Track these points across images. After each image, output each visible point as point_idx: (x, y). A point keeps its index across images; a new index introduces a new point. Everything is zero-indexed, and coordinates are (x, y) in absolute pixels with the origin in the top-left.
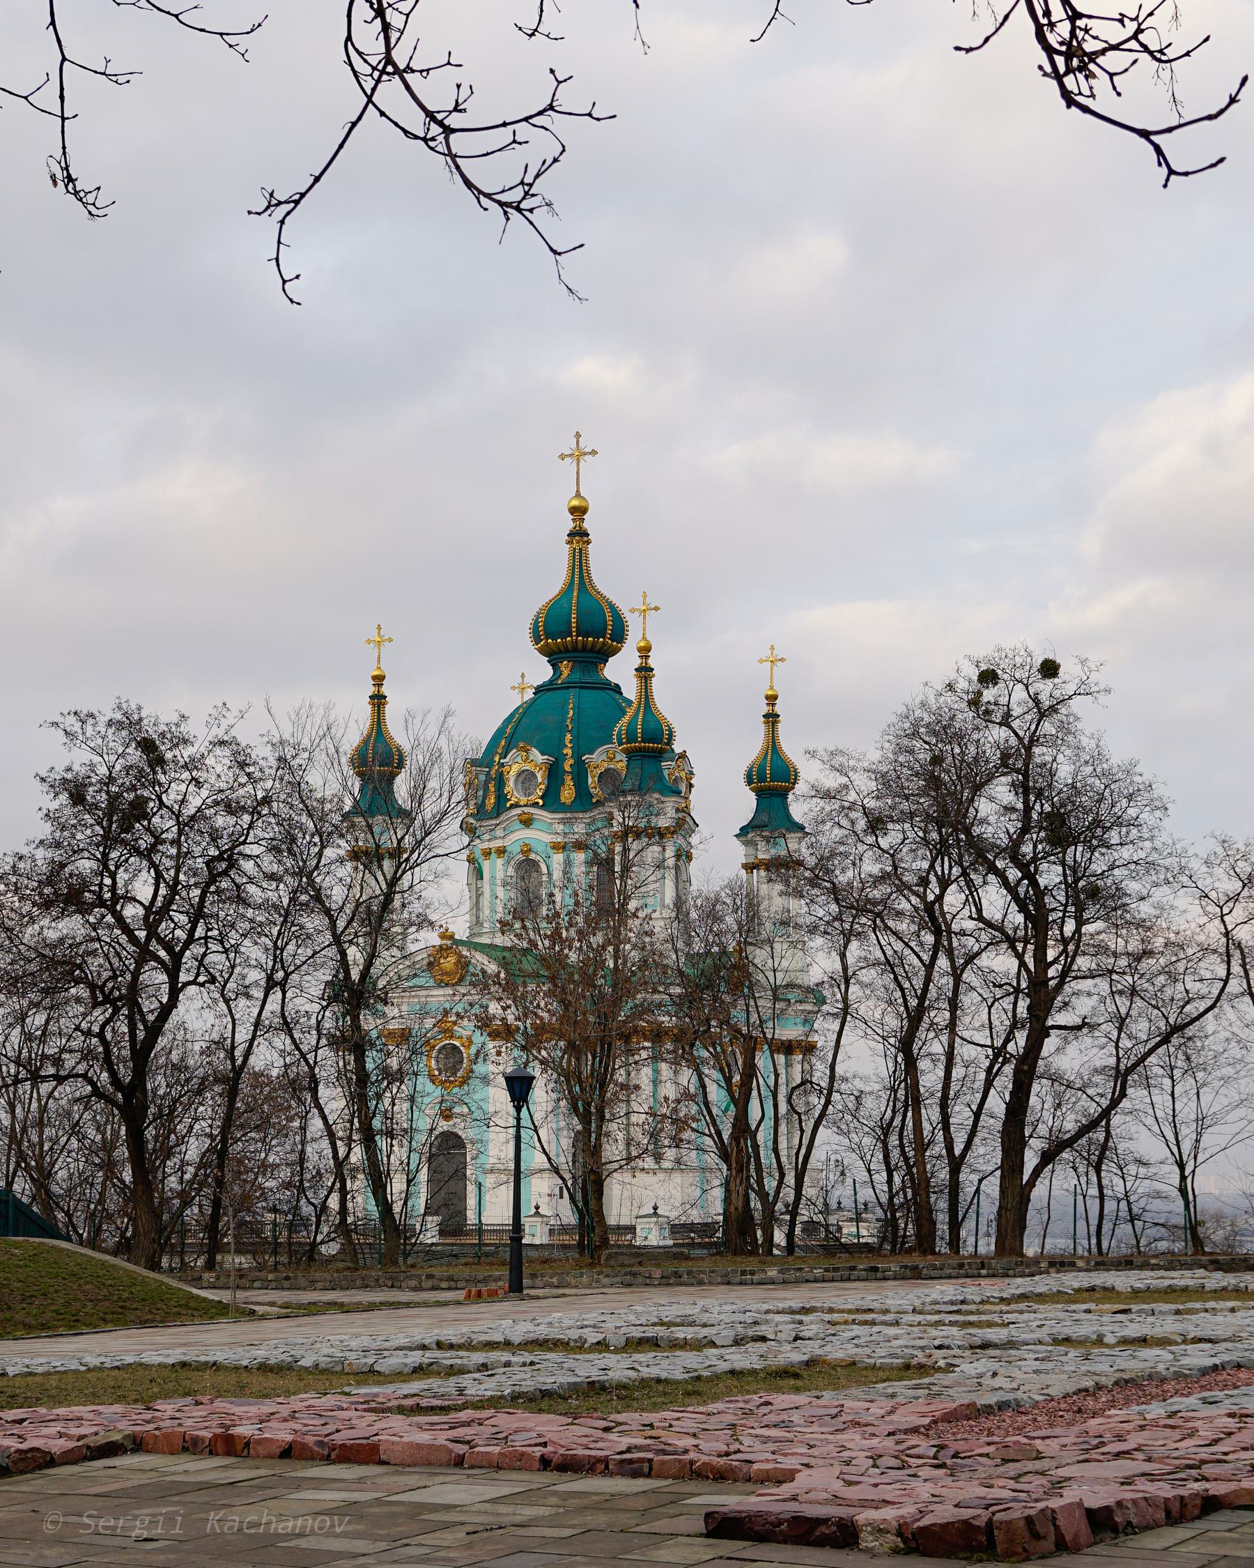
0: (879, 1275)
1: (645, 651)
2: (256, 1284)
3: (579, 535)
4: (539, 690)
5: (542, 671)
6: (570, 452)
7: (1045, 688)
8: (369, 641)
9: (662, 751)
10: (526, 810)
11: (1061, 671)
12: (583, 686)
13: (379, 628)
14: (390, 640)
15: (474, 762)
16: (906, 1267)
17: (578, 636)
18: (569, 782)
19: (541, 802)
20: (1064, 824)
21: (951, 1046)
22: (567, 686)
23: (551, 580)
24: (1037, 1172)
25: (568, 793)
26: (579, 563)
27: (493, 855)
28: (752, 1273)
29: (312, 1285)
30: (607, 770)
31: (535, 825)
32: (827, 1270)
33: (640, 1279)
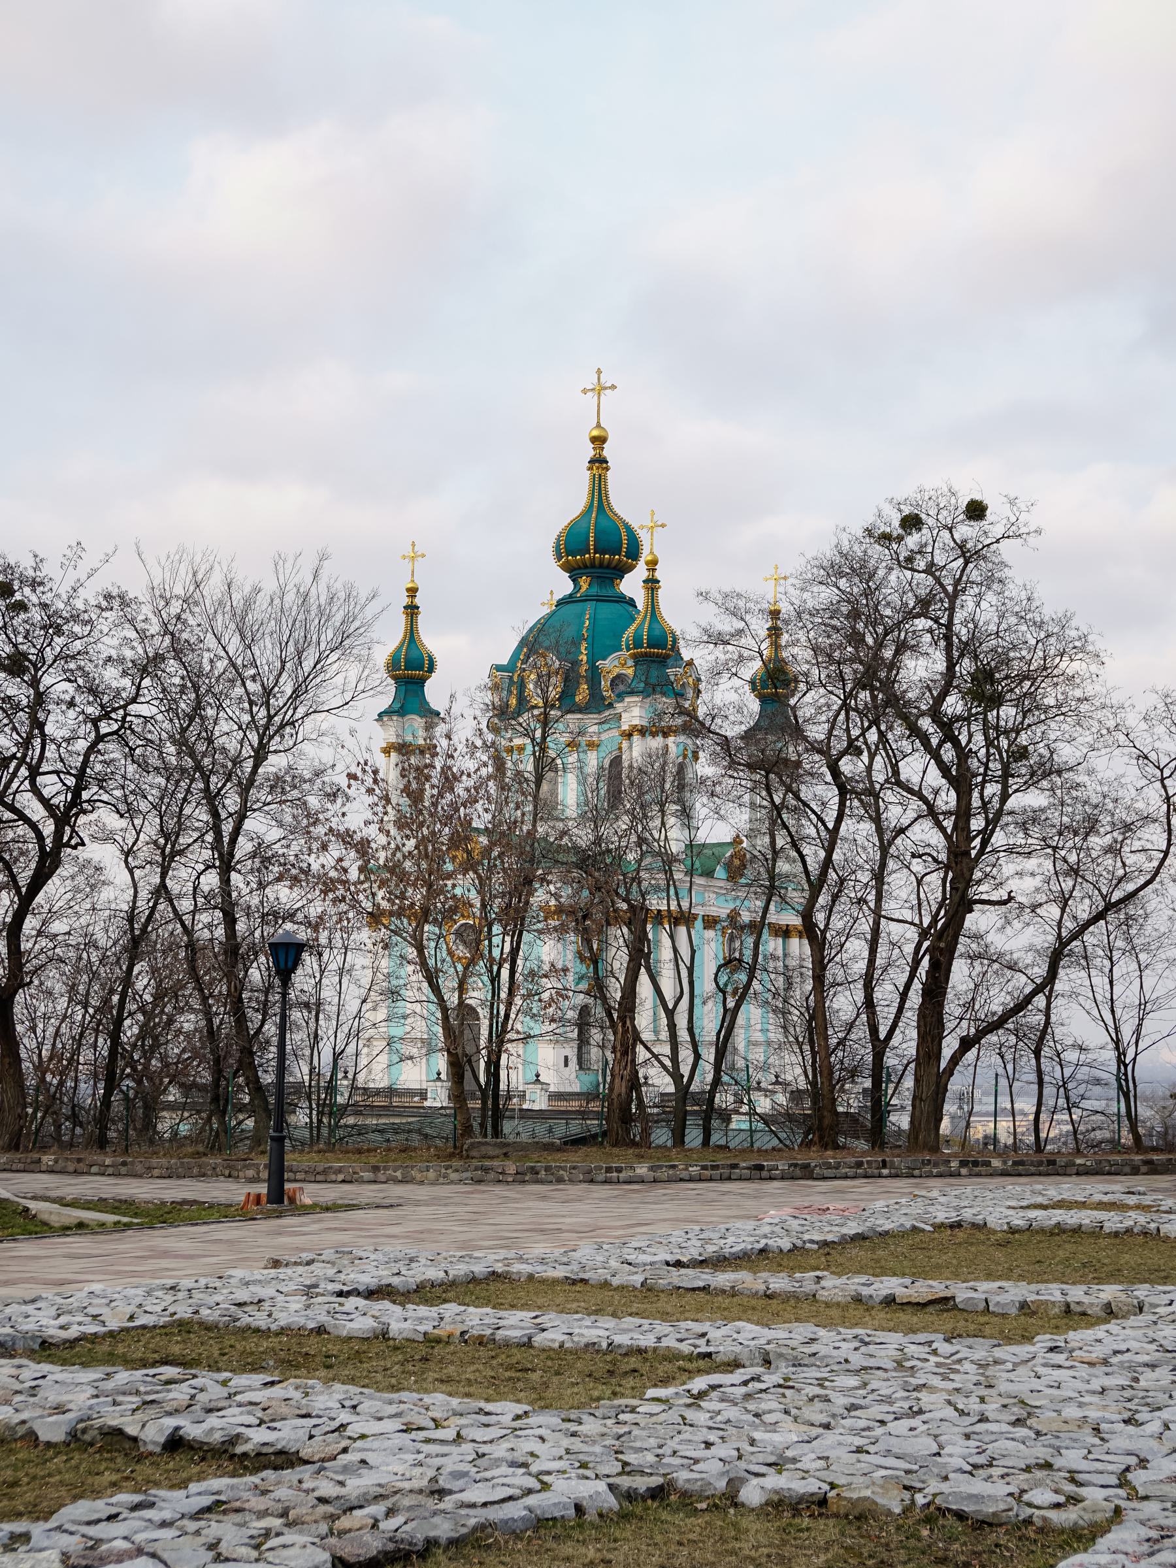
0: (765, 1174)
1: (652, 564)
2: (94, 1169)
3: (599, 462)
4: (561, 603)
5: (564, 585)
7: (967, 531)
8: (404, 557)
9: (667, 656)
11: (988, 512)
12: (599, 599)
13: (413, 544)
14: (423, 556)
15: (499, 668)
16: (796, 1165)
20: (988, 682)
21: (877, 924)
22: (585, 599)
24: (955, 1060)
25: (582, 693)
26: (599, 489)
28: (619, 1170)
29: (147, 1173)
32: (704, 1168)
33: (492, 1175)
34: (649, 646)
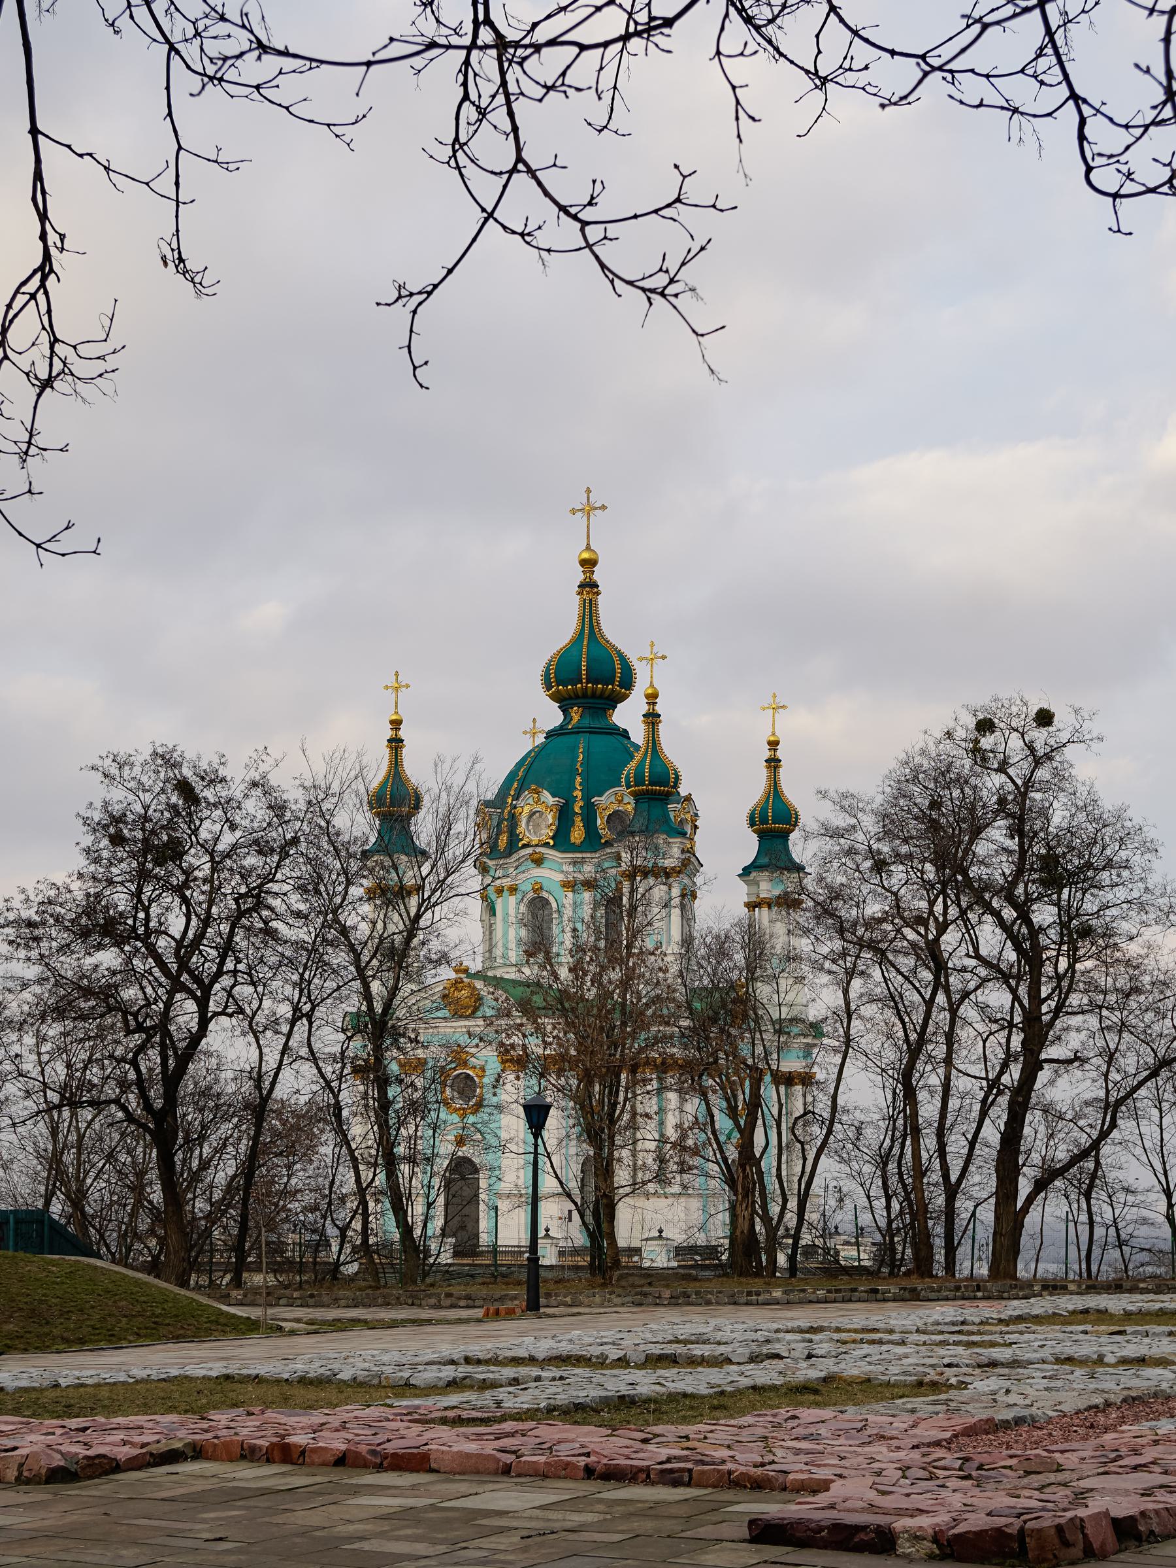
0: (879, 1296)
1: (652, 698)
2: (282, 1302)
3: (589, 587)
4: (550, 735)
5: (553, 716)
6: (581, 507)
7: (1039, 736)
8: (387, 687)
9: (668, 794)
10: (538, 850)
11: (1056, 719)
12: (592, 731)
13: (397, 674)
14: (407, 686)
15: (487, 804)
16: (905, 1289)
17: (587, 683)
18: (579, 823)
19: (552, 843)
20: (1058, 867)
21: (948, 1078)
22: (577, 731)
23: (563, 628)
24: (1030, 1200)
25: (577, 834)
27: (506, 893)
28: (758, 1294)
29: (335, 1302)
30: (615, 812)
31: (546, 864)
32: (829, 1291)
33: (650, 1299)
34: (649, 784)
